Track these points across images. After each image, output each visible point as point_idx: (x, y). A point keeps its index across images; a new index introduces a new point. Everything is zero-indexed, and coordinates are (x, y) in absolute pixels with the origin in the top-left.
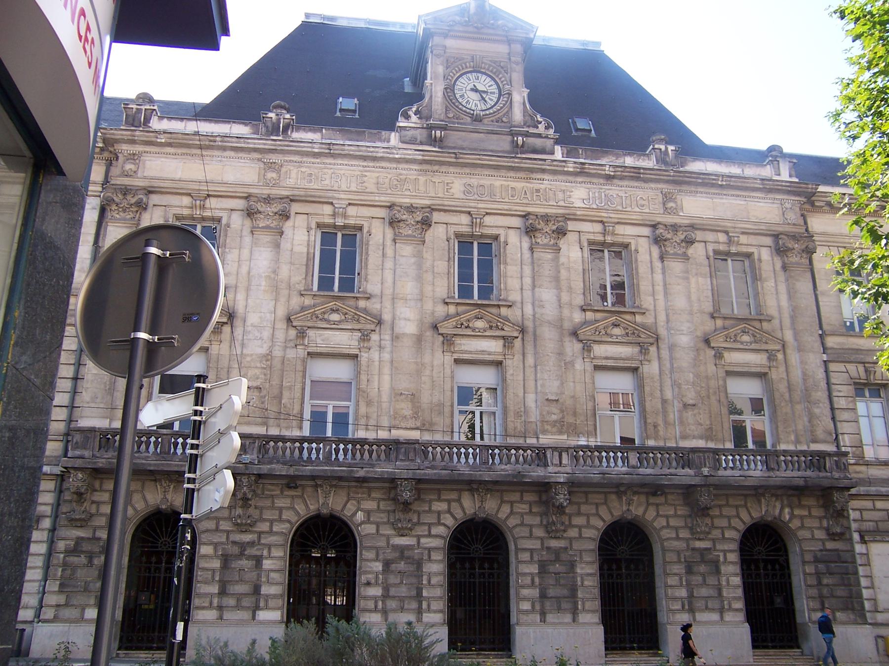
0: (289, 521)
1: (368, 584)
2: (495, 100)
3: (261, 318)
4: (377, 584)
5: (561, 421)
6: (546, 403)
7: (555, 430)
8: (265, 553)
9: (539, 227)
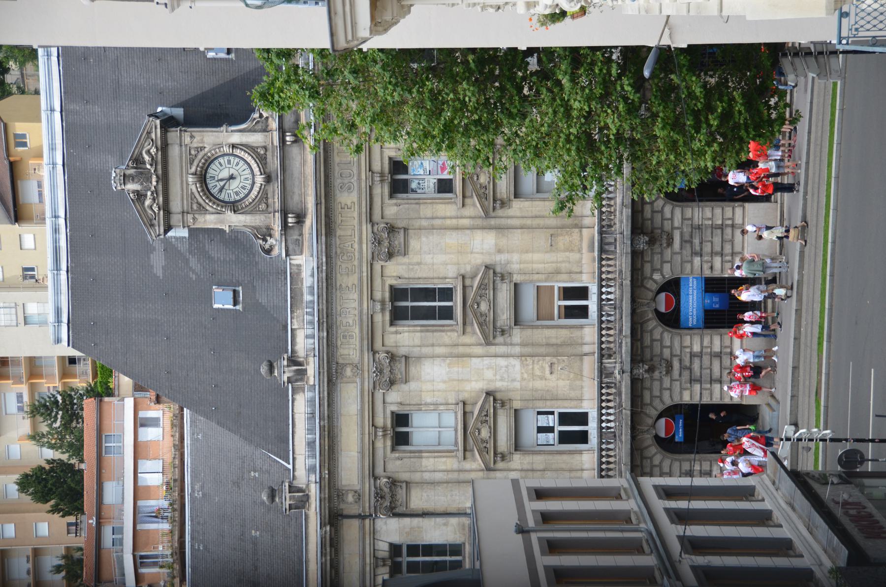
0: (662, 334)
1: (712, 268)
2: (237, 160)
3: (488, 368)
4: (712, 262)
8: (688, 350)
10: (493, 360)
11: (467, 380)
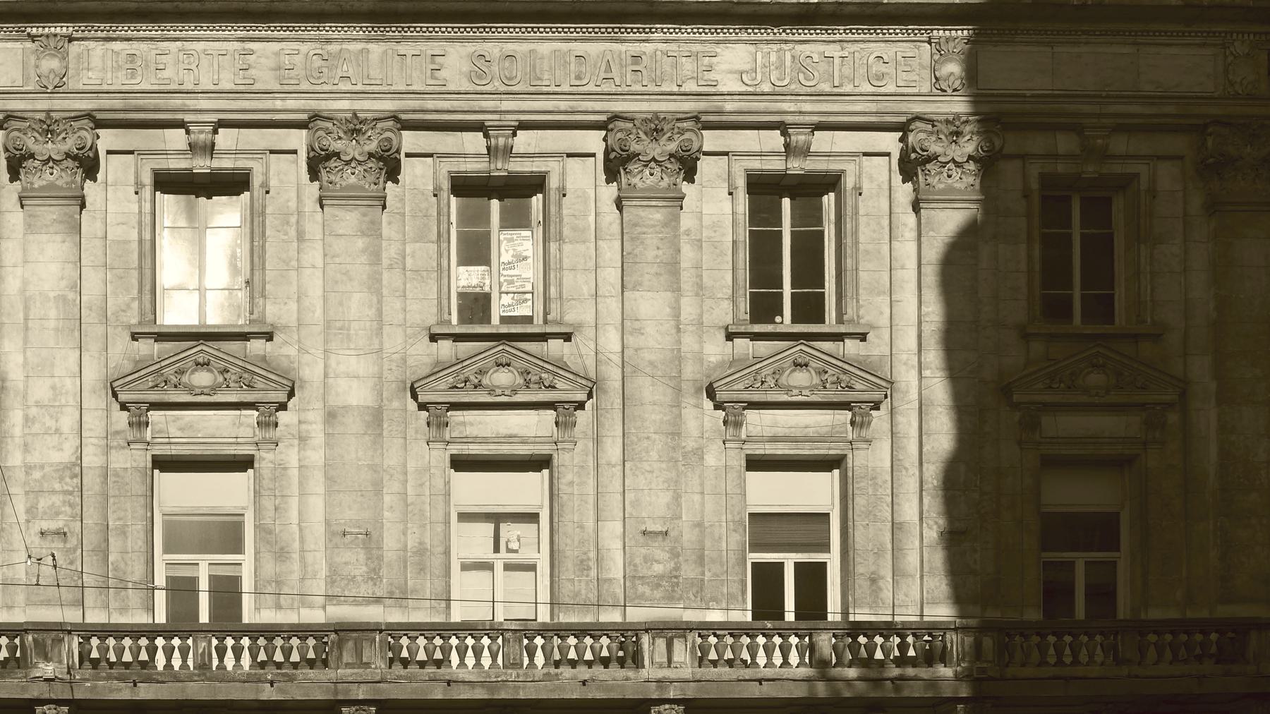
3: (53, 388)
5: (673, 576)
6: (641, 539)
7: (658, 594)
9: (635, 147)
10: (73, 401)
11: (26, 341)
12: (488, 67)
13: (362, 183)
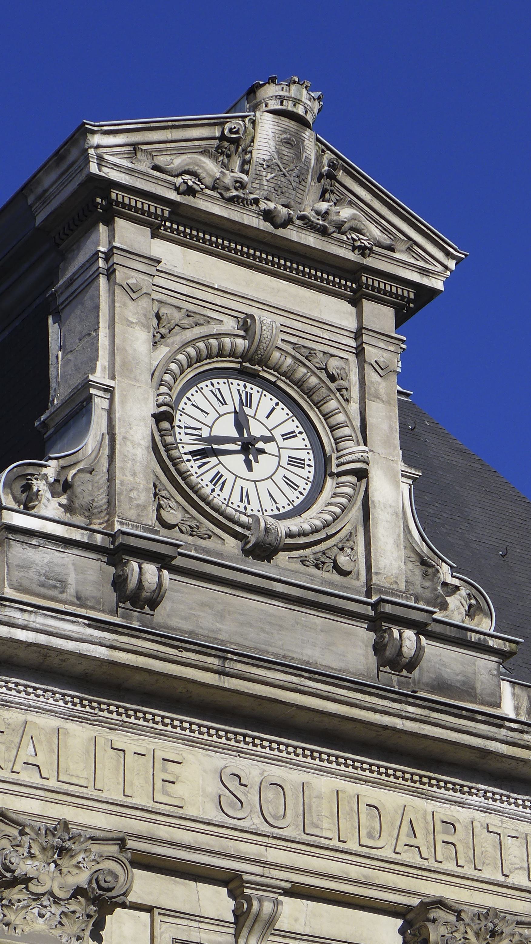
12: (245, 795)
13: (56, 932)
